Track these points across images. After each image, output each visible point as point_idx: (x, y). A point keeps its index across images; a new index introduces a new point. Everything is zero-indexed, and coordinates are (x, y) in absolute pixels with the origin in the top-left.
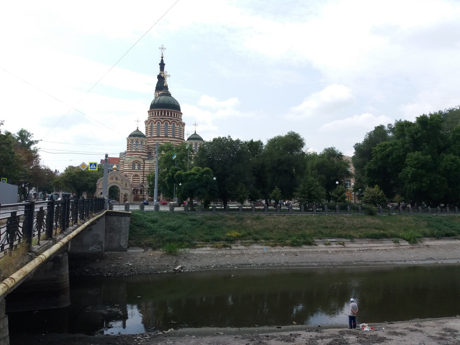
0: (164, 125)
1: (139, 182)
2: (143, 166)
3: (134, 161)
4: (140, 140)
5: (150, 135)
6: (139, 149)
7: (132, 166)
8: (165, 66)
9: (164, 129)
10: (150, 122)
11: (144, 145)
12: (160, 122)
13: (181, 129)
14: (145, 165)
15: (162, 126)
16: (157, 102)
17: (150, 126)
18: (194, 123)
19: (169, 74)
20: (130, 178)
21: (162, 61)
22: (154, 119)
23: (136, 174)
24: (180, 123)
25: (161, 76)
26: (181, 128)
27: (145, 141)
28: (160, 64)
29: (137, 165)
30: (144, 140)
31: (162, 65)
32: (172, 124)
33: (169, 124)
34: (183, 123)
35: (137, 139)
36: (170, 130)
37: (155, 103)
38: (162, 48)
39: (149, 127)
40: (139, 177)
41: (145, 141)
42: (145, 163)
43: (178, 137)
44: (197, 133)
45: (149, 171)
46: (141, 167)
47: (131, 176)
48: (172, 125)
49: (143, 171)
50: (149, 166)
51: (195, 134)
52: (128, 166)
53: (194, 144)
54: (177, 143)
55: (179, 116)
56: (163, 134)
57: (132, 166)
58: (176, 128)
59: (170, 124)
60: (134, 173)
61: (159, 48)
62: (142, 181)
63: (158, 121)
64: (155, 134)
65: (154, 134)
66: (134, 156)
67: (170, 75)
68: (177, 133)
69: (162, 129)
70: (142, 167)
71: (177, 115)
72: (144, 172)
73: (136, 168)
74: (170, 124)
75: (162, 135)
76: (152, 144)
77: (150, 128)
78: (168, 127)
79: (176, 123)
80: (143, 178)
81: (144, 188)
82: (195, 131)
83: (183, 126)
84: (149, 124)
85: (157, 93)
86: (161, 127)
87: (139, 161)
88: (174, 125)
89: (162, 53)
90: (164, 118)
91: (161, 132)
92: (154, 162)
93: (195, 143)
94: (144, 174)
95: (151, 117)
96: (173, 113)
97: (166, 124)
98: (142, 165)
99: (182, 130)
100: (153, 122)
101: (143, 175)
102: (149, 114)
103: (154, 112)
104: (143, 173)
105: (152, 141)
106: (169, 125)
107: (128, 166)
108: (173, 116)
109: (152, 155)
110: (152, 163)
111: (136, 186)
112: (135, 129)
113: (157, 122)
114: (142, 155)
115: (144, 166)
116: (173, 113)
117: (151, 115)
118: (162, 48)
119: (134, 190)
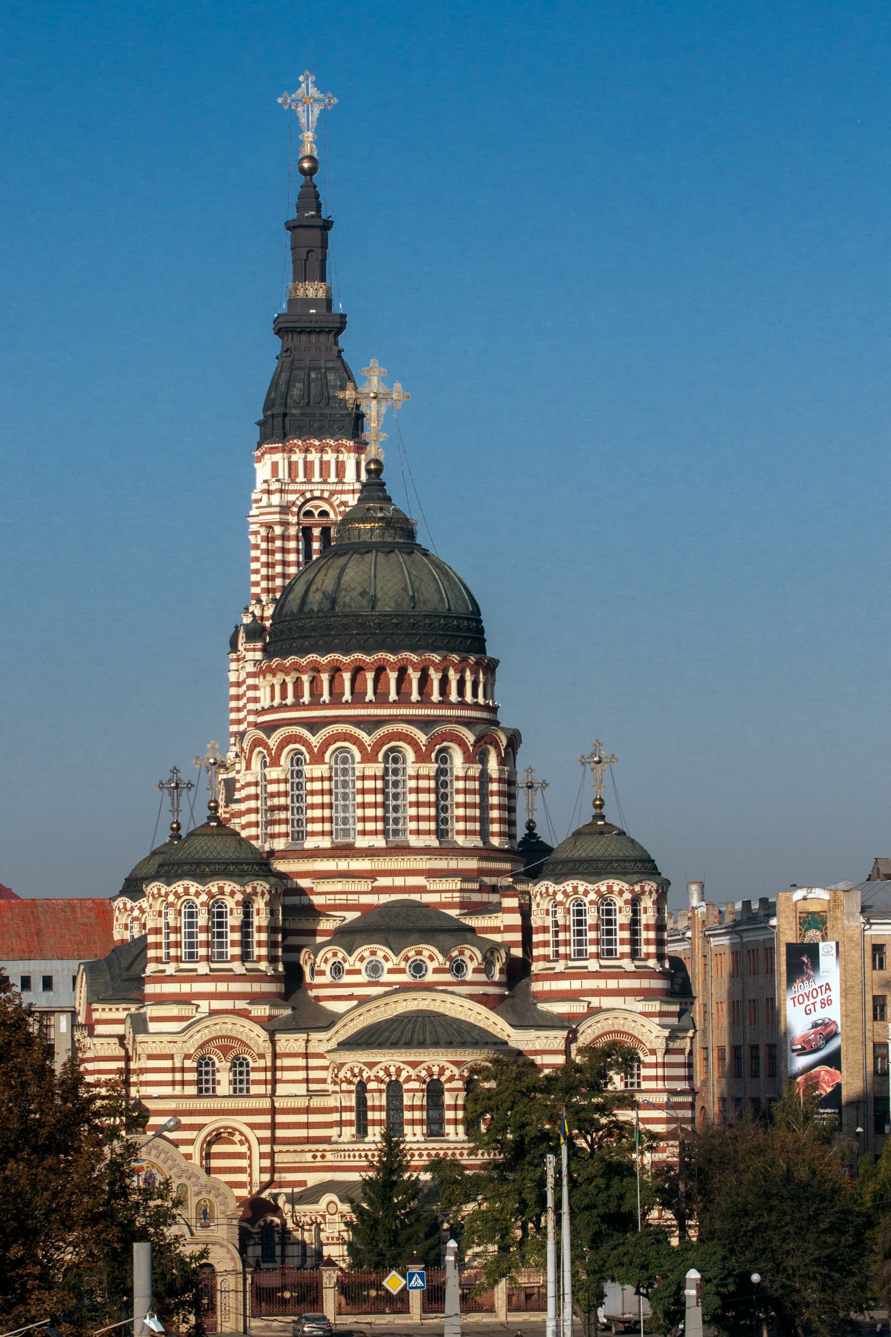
1: (243, 1178)
2: (265, 1069)
3: (205, 1039)
5: (286, 835)
7: (193, 1076)
10: (281, 747)
12: (354, 749)
14: (279, 1063)
15: (368, 772)
16: (327, 605)
17: (282, 777)
22: (313, 726)
23: (226, 1128)
25: (344, 401)
28: (291, 227)
29: (229, 1064)
32: (433, 755)
33: (411, 756)
37: (306, 609)
39: (278, 781)
40: (244, 1149)
42: (278, 1051)
44: (612, 816)
45: (302, 1103)
46: (254, 1076)
47: (191, 1142)
49: (266, 1103)
50: (307, 1068)
52: (168, 1077)
56: (376, 833)
57: (193, 1076)
59: (422, 757)
60: (213, 1123)
62: (262, 1170)
63: (339, 744)
64: (323, 833)
65: (313, 834)
66: (204, 1005)
70: (261, 1076)
72: (273, 1111)
73: (224, 1088)
74: (424, 761)
75: (367, 837)
80: (272, 1155)
84: (275, 762)
85: (278, 457)
86: (359, 784)
87: (242, 1042)
90: (380, 722)
91: (364, 819)
92: (333, 1044)
94: (273, 1126)
95: (283, 707)
98: (261, 1063)
100: (303, 749)
101: (267, 1133)
103: (305, 678)
104: (267, 1119)
107: (168, 1077)
108: (436, 697)
109: (313, 993)
110: (322, 1048)
113: (332, 748)
115: (274, 1069)
117: (284, 696)
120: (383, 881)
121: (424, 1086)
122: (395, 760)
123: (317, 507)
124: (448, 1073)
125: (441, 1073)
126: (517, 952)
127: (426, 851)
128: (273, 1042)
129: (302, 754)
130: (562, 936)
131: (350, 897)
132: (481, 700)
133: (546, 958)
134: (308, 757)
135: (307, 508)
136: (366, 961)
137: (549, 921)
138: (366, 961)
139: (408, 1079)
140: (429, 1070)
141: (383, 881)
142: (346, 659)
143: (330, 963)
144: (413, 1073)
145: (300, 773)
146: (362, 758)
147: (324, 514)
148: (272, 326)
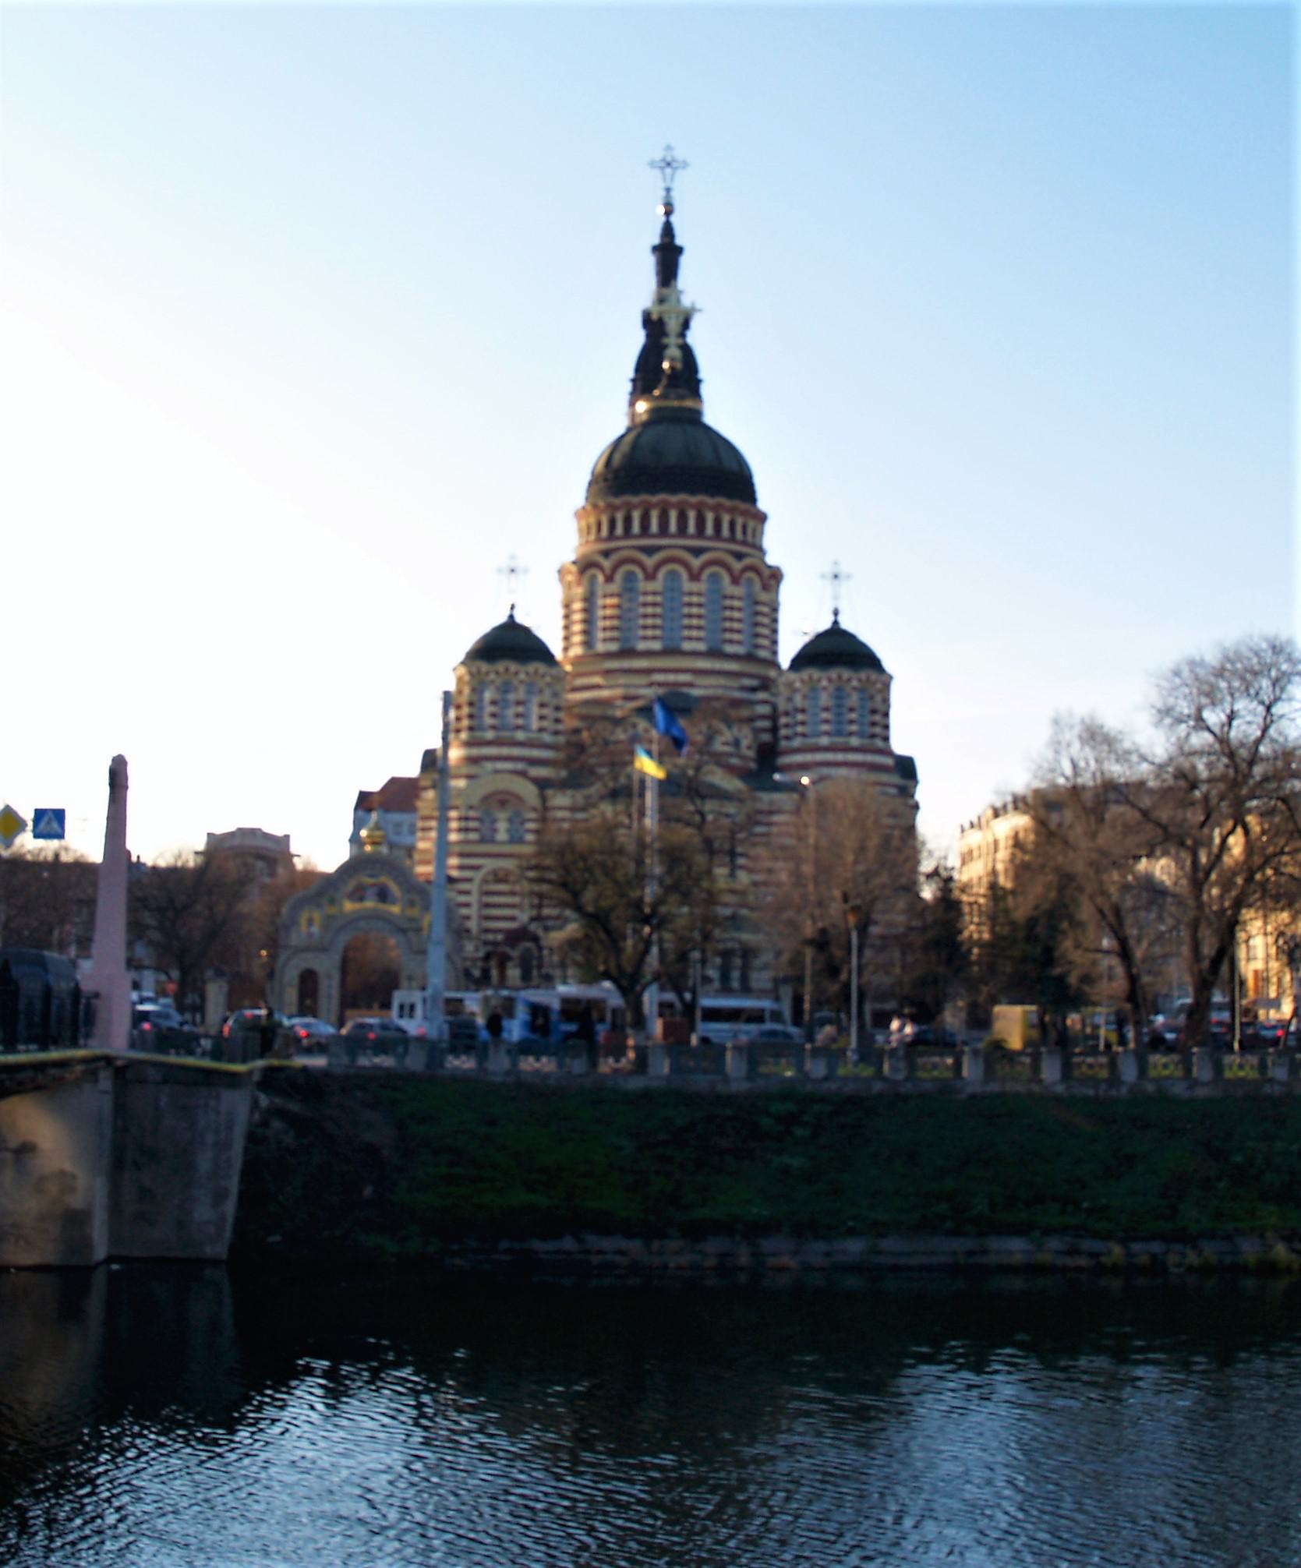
0: (658, 585)
4: (522, 676)
6: (518, 727)
13: (757, 603)
18: (829, 569)
20: (467, 893)
21: (668, 231)
24: (751, 568)
27: (548, 679)
28: (655, 249)
31: (668, 255)
33: (685, 575)
34: (770, 567)
35: (507, 670)
38: (663, 160)
43: (740, 650)
44: (846, 624)
47: (469, 880)
48: (702, 586)
51: (836, 633)
53: (825, 688)
55: (744, 532)
56: (654, 638)
58: (728, 602)
59: (695, 577)
60: (489, 864)
61: (652, 164)
66: (489, 766)
68: (736, 625)
70: (531, 826)
71: (732, 525)
73: (502, 836)
79: (728, 569)
81: (540, 949)
82: (836, 613)
89: (668, 190)
90: (658, 549)
93: (830, 680)
96: (710, 517)
97: (673, 575)
99: (765, 609)
102: (580, 530)
105: (597, 680)
106: (687, 585)
108: (709, 530)
111: (500, 937)
112: (502, 619)
114: (534, 762)
118: (669, 164)
119: (487, 957)
126: (766, 737)
127: (694, 654)
128: (544, 799)
133: (787, 738)
137: (789, 707)
142: (635, 500)
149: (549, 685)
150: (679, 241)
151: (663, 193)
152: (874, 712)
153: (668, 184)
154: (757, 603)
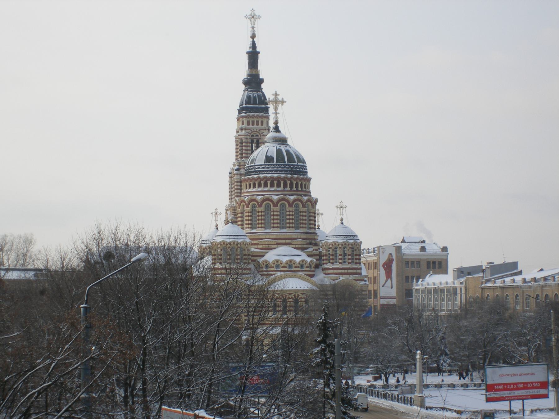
0: (278, 209)
8: (260, 56)
9: (278, 217)
11: (245, 255)
13: (310, 213)
15: (275, 210)
19: (283, 99)
21: (254, 46)
26: (311, 211)
27: (247, 246)
28: (248, 53)
30: (246, 245)
33: (287, 205)
36: (291, 217)
38: (251, 15)
39: (248, 212)
41: (247, 246)
54: (305, 243)
55: (305, 188)
58: (302, 214)
59: (290, 206)
61: (246, 17)
67: (284, 100)
68: (304, 222)
69: (275, 217)
71: (301, 184)
76: (256, 246)
77: (250, 214)
78: (287, 212)
82: (342, 220)
83: (313, 207)
86: (272, 213)
88: (297, 207)
89: (253, 28)
96: (294, 183)
97: (283, 205)
99: (313, 215)
100: (256, 203)
106: (288, 209)
108: (294, 189)
116: (294, 183)
118: (253, 17)
120: (280, 241)
121: (293, 300)
122: (283, 206)
123: (255, 134)
124: (300, 297)
125: (298, 297)
129: (256, 204)
130: (331, 257)
131: (269, 246)
132: (308, 190)
134: (257, 205)
135: (252, 134)
136: (275, 264)
138: (275, 264)
139: (289, 298)
140: (294, 295)
141: (280, 241)
143: (265, 265)
144: (290, 296)
145: (255, 210)
146: (273, 205)
147: (257, 136)
148: (242, 82)
149: (247, 247)
150: (258, 50)
151: (251, 29)
152: (356, 255)
153: (253, 25)
154: (310, 213)
